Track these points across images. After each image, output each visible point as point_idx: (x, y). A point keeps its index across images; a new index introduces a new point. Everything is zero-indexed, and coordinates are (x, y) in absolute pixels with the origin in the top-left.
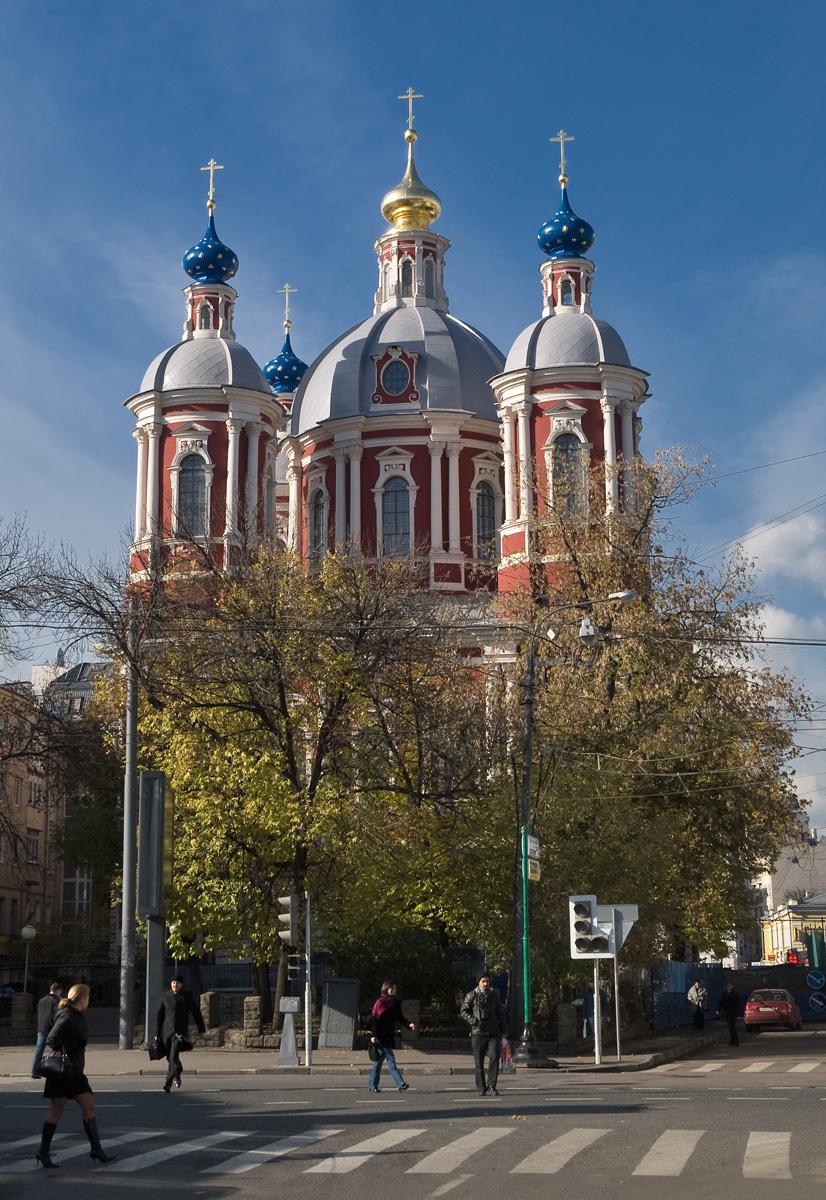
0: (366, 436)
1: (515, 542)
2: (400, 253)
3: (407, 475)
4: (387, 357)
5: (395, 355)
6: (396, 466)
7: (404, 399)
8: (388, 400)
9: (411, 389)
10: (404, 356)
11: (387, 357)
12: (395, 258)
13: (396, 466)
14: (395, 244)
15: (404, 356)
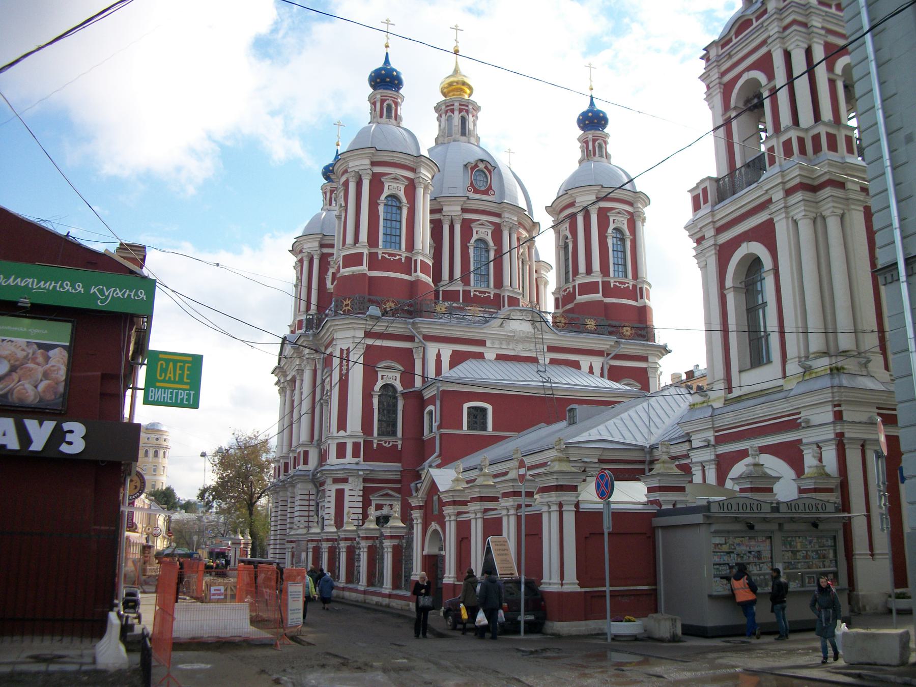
0: (464, 210)
1: (589, 288)
2: (460, 111)
3: (489, 239)
4: (476, 166)
5: (481, 166)
6: (482, 232)
7: (486, 192)
8: (476, 191)
9: (490, 188)
10: (486, 167)
11: (476, 166)
12: (456, 113)
13: (482, 232)
14: (457, 104)
15: (486, 167)
